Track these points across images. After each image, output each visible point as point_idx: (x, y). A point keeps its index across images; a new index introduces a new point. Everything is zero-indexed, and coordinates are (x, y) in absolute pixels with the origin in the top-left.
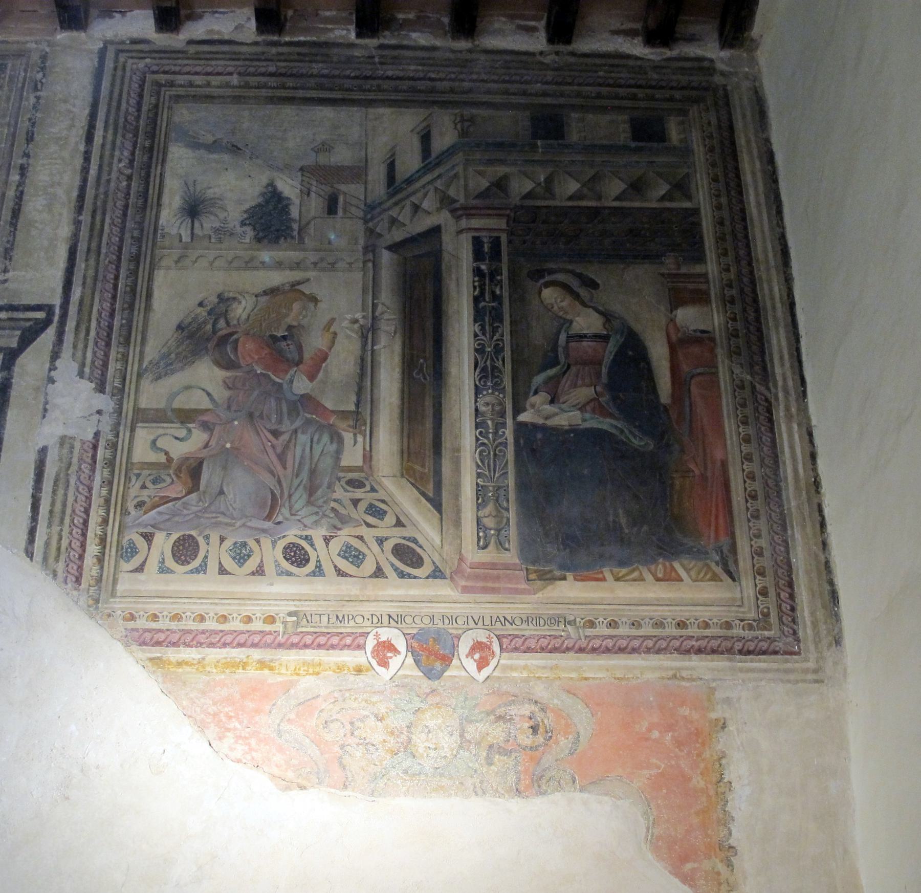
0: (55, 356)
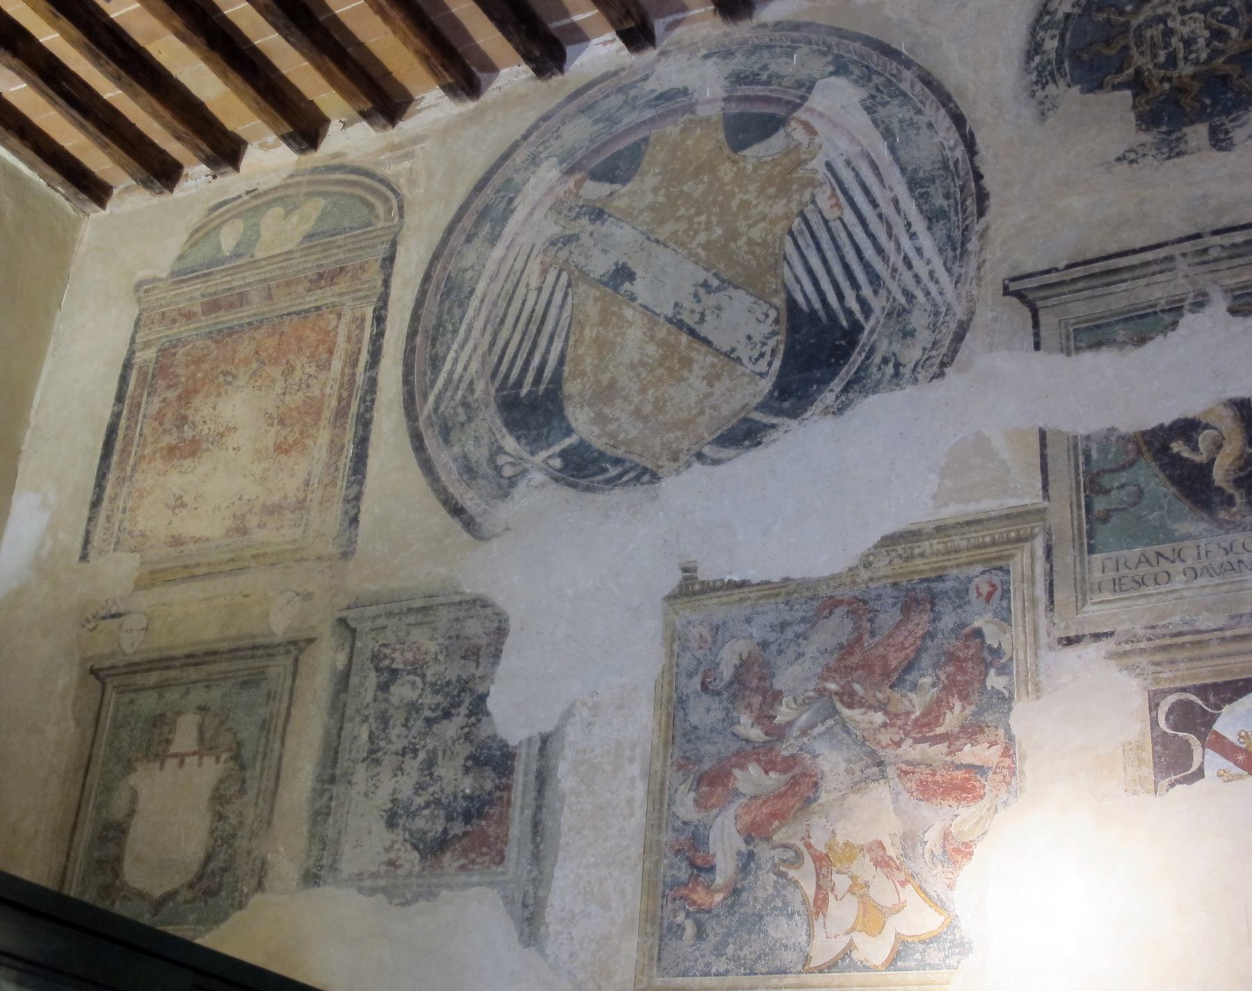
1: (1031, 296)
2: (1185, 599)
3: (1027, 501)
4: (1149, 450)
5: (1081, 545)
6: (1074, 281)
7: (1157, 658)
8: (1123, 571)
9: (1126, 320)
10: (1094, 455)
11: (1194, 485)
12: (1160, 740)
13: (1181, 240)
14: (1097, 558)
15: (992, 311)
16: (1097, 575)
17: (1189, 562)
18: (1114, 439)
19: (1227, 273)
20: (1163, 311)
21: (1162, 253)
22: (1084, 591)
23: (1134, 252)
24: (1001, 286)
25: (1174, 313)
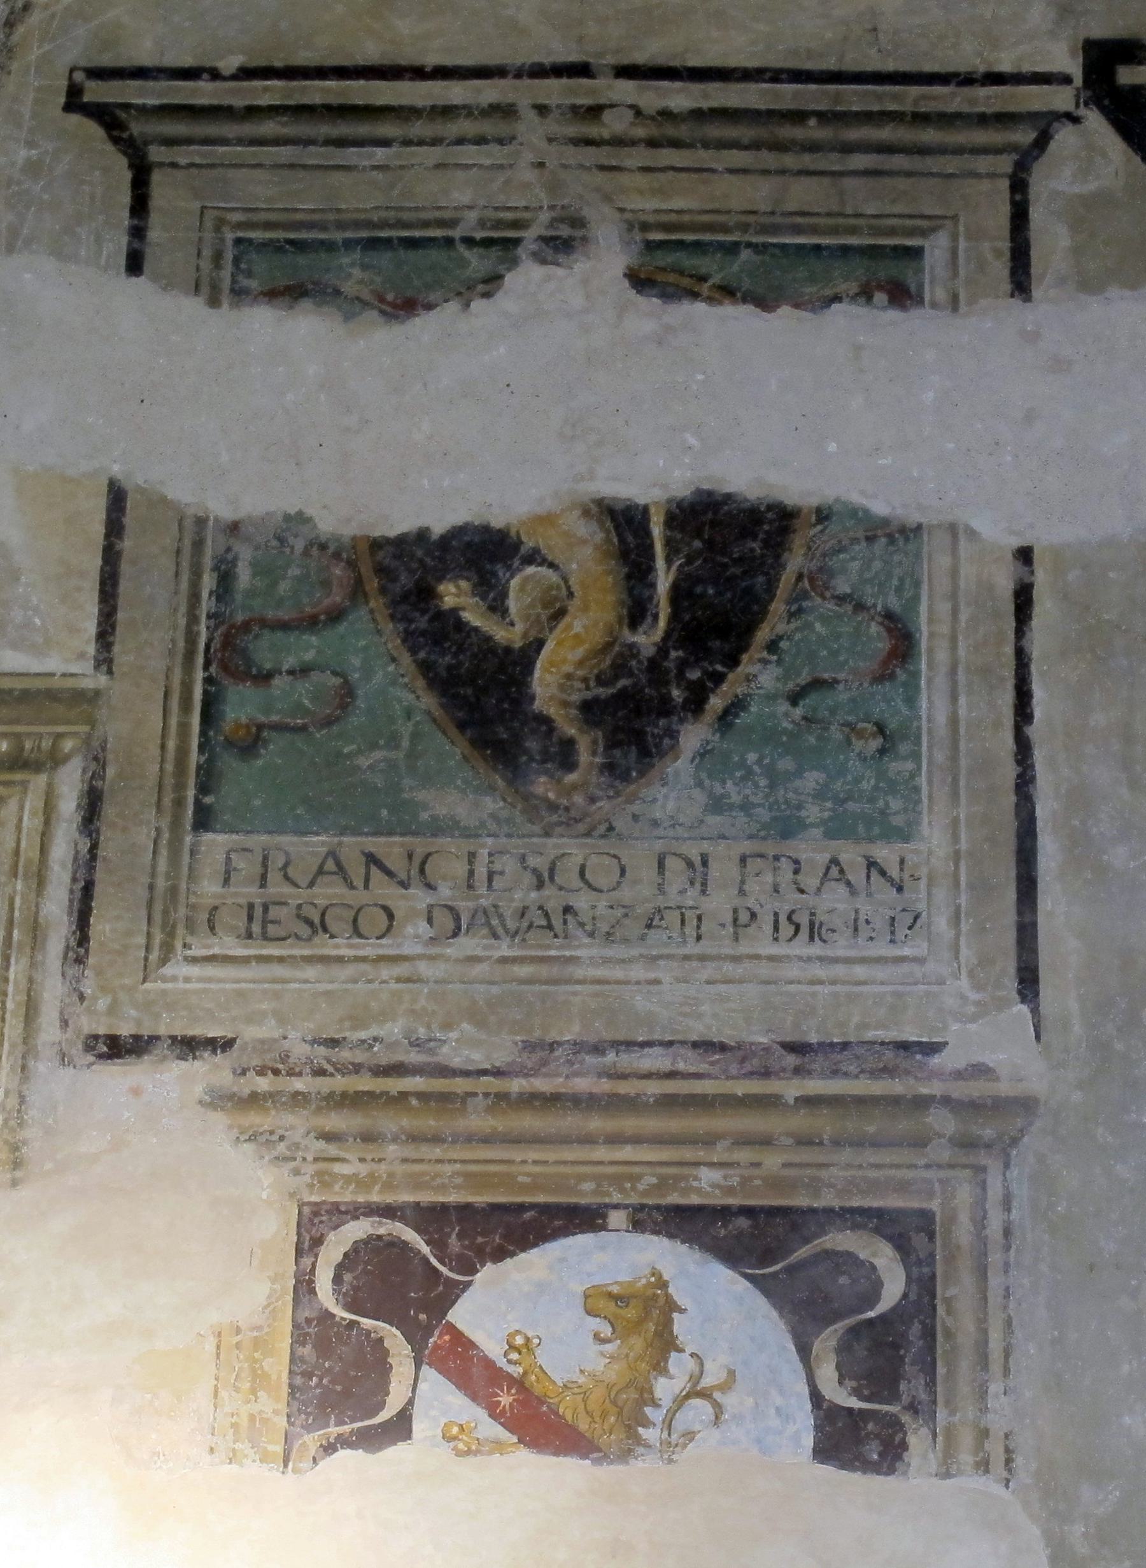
1: (137, 128)
2: (420, 984)
3: (53, 663)
4: (383, 590)
5: (179, 803)
6: (252, 112)
7: (335, 1121)
8: (277, 888)
9: (373, 244)
10: (244, 576)
11: (483, 698)
12: (315, 1332)
13: (539, 72)
14: (216, 842)
15: (30, 144)
16: (209, 888)
17: (445, 892)
18: (299, 545)
19: (641, 180)
20: (469, 241)
21: (489, 92)
22: (170, 921)
23: (419, 73)
24: (64, 83)
25: (495, 252)
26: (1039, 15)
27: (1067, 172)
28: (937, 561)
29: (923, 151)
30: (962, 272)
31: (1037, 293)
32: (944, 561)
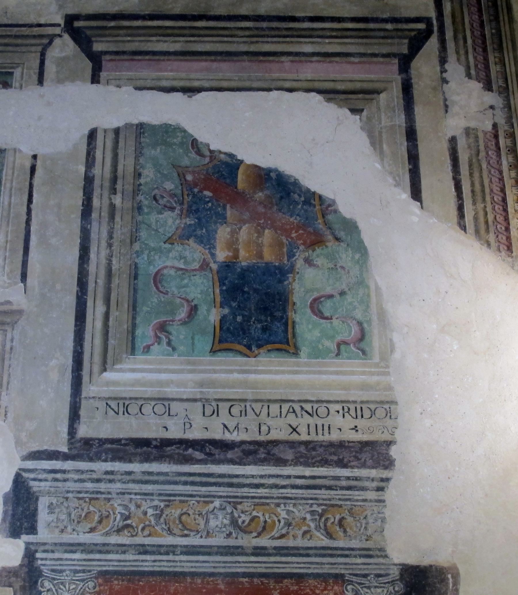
0: (443, 61)
26: (54, 8)
27: (57, 50)
28: (9, 158)
29: (17, 45)
30: (24, 79)
31: (45, 84)
32: (11, 159)
